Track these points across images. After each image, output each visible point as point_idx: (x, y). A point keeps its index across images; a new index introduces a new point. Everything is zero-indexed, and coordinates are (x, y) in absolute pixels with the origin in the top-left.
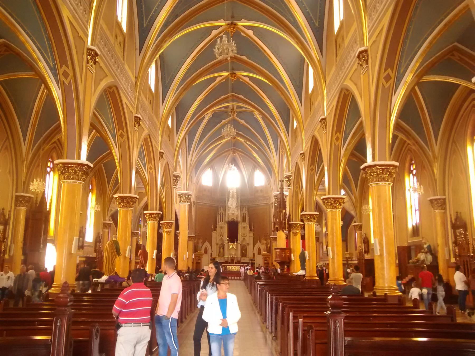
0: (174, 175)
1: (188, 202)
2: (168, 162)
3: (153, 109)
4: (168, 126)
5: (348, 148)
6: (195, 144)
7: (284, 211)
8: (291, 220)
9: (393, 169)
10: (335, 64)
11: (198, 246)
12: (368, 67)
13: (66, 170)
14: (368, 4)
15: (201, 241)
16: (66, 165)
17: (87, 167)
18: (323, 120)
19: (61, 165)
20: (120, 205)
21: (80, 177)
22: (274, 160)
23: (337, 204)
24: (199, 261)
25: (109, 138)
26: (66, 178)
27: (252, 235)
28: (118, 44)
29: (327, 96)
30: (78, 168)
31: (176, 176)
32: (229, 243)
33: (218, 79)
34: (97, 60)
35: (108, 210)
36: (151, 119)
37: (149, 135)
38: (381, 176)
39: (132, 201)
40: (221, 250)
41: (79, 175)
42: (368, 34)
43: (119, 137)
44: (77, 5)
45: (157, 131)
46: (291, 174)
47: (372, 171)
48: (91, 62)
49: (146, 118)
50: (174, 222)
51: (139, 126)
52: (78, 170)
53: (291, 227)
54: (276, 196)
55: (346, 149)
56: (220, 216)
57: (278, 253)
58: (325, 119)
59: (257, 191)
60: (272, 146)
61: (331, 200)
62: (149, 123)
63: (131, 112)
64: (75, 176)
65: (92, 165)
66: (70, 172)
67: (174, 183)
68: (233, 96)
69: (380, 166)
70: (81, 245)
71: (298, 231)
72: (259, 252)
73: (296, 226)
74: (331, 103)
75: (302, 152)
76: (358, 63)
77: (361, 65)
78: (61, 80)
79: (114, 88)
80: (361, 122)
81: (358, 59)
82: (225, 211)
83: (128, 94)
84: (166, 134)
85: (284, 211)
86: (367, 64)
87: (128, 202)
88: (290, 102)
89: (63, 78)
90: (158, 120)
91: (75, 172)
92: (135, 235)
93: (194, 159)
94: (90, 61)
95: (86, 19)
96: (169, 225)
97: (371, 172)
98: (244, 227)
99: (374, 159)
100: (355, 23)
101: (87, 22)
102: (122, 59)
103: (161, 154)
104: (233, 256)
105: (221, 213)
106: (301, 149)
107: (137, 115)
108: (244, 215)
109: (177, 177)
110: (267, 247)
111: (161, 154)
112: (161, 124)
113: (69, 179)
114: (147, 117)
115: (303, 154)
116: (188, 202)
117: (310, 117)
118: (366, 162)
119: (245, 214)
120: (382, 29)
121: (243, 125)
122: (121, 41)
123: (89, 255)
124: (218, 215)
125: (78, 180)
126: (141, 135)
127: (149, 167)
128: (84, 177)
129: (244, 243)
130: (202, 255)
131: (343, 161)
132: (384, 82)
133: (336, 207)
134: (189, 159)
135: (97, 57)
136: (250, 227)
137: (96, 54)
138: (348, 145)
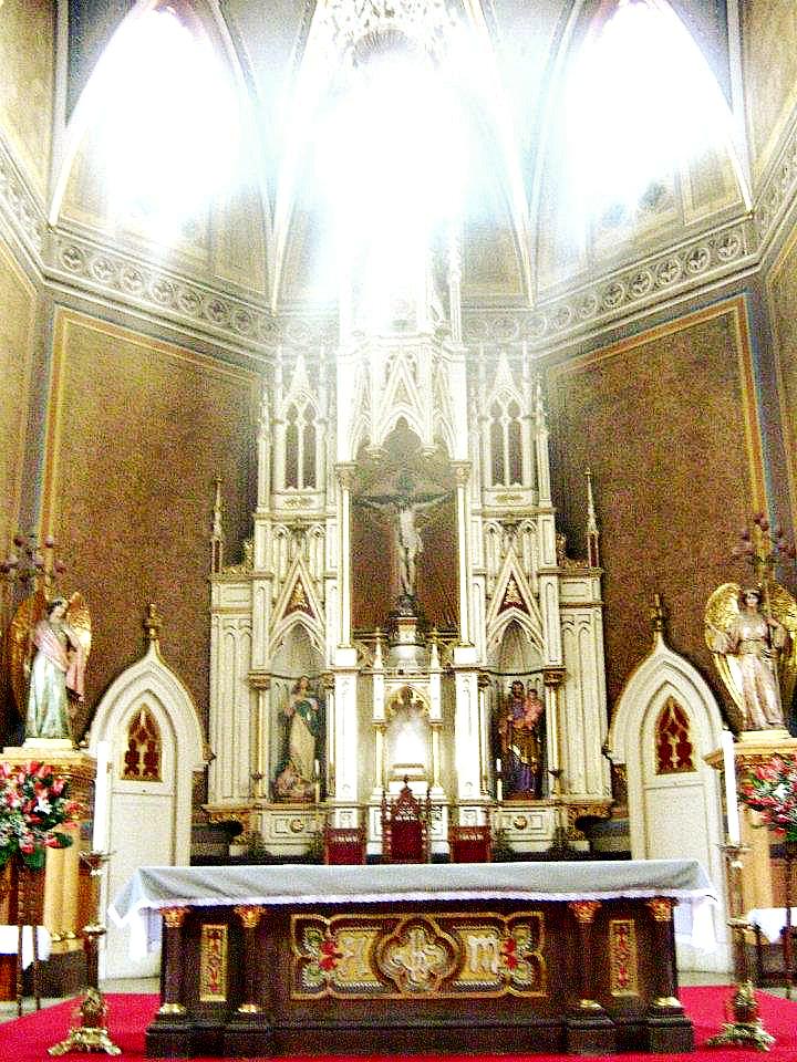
15: (83, 638)
27: (587, 589)
40: (301, 740)
56: (281, 430)
82: (332, 386)
104: (406, 793)
105: (292, 414)
124: (265, 427)
136: (567, 526)
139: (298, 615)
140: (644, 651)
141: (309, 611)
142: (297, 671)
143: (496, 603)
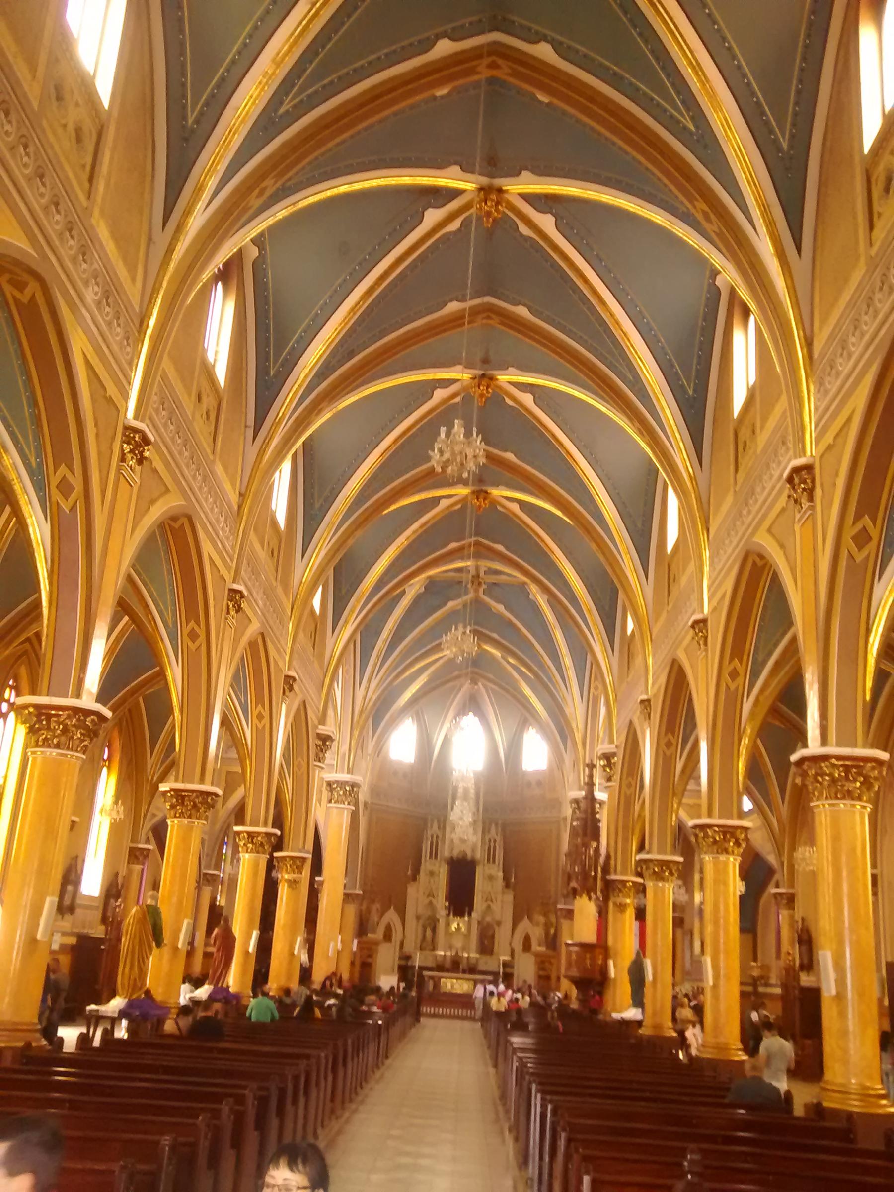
0: (318, 734)
1: (349, 804)
2: (304, 702)
3: (277, 571)
4: (312, 611)
5: (761, 698)
6: (378, 657)
7: (594, 845)
8: (612, 870)
9: (873, 768)
10: (732, 489)
11: (367, 920)
12: (812, 508)
13: (44, 722)
14: (816, 355)
16: (44, 711)
17: (95, 718)
18: (700, 625)
19: (31, 710)
20: (172, 812)
21: (77, 742)
22: (576, 709)
23: (729, 841)
24: (370, 960)
25: (162, 640)
26: (40, 743)
27: (509, 897)
28: (202, 416)
29: (711, 565)
30: (74, 720)
31: (323, 737)
32: (449, 915)
33: (444, 503)
34: (146, 454)
35: (145, 815)
36: (269, 594)
37: (262, 634)
38: (843, 786)
39: (204, 802)
40: (429, 933)
41: (75, 737)
42: (815, 428)
43: (186, 639)
44: (109, 324)
45: (283, 624)
46: (615, 750)
47: (819, 771)
48: (132, 458)
49: (257, 593)
50: (310, 856)
51: (237, 612)
52: (74, 725)
53: (610, 887)
54: (576, 801)
55: (757, 701)
57: (574, 956)
58: (704, 621)
59: (529, 784)
60: (571, 674)
61: (715, 831)
62: (265, 605)
63: (222, 577)
64: (63, 738)
65: (108, 714)
66: (52, 727)
67: (317, 755)
68: (477, 544)
69: (839, 758)
70: (67, 902)
71: (628, 901)
72: (527, 945)
73: (625, 886)
74: (720, 585)
75: (644, 697)
76: (789, 497)
77: (796, 501)
78: (53, 499)
79: (185, 521)
80: (794, 639)
81: (788, 486)
83: (217, 535)
84: (304, 630)
85: (594, 845)
86: (811, 499)
87: (195, 806)
88: (618, 571)
89: (56, 496)
90: (288, 599)
91: (65, 730)
92: (208, 881)
93: (373, 695)
94: (129, 456)
95: (128, 357)
96: (297, 864)
97: (817, 774)
98: (491, 878)
99: (824, 741)
100: (784, 397)
101: (130, 363)
102: (209, 451)
103: (289, 682)
104: (457, 953)
106: (643, 688)
107: (236, 586)
108: (492, 844)
109: (325, 740)
110: (547, 934)
111: (289, 682)
112: (295, 607)
113: (49, 746)
114: (262, 590)
115: (646, 703)
116: (349, 804)
117: (668, 612)
118: (805, 745)
119: (495, 841)
120: (849, 420)
121: (500, 616)
122: (211, 408)
123: (86, 931)
125: (72, 750)
126: (243, 634)
127: (255, 713)
128: (86, 743)
129: (488, 919)
130: (377, 943)
131: (749, 731)
132: (854, 549)
133: (726, 851)
134: (360, 694)
135: (146, 448)
136: (506, 878)
137: (146, 441)
138: (762, 691)
139: (431, 898)
140: (521, 919)
141: (434, 897)
142: (429, 913)
143: (485, 899)
